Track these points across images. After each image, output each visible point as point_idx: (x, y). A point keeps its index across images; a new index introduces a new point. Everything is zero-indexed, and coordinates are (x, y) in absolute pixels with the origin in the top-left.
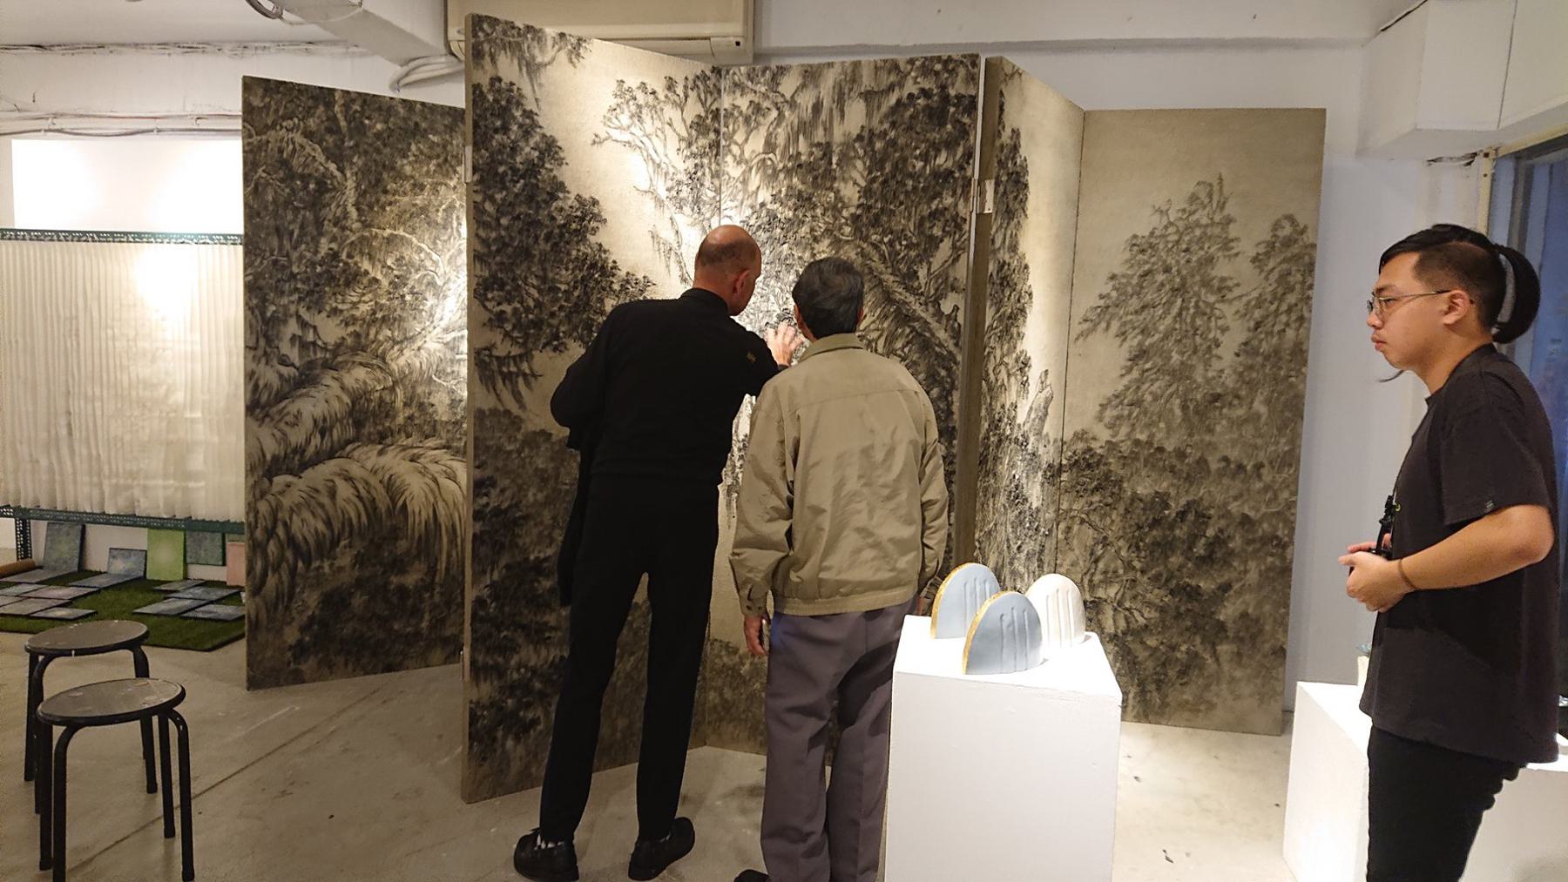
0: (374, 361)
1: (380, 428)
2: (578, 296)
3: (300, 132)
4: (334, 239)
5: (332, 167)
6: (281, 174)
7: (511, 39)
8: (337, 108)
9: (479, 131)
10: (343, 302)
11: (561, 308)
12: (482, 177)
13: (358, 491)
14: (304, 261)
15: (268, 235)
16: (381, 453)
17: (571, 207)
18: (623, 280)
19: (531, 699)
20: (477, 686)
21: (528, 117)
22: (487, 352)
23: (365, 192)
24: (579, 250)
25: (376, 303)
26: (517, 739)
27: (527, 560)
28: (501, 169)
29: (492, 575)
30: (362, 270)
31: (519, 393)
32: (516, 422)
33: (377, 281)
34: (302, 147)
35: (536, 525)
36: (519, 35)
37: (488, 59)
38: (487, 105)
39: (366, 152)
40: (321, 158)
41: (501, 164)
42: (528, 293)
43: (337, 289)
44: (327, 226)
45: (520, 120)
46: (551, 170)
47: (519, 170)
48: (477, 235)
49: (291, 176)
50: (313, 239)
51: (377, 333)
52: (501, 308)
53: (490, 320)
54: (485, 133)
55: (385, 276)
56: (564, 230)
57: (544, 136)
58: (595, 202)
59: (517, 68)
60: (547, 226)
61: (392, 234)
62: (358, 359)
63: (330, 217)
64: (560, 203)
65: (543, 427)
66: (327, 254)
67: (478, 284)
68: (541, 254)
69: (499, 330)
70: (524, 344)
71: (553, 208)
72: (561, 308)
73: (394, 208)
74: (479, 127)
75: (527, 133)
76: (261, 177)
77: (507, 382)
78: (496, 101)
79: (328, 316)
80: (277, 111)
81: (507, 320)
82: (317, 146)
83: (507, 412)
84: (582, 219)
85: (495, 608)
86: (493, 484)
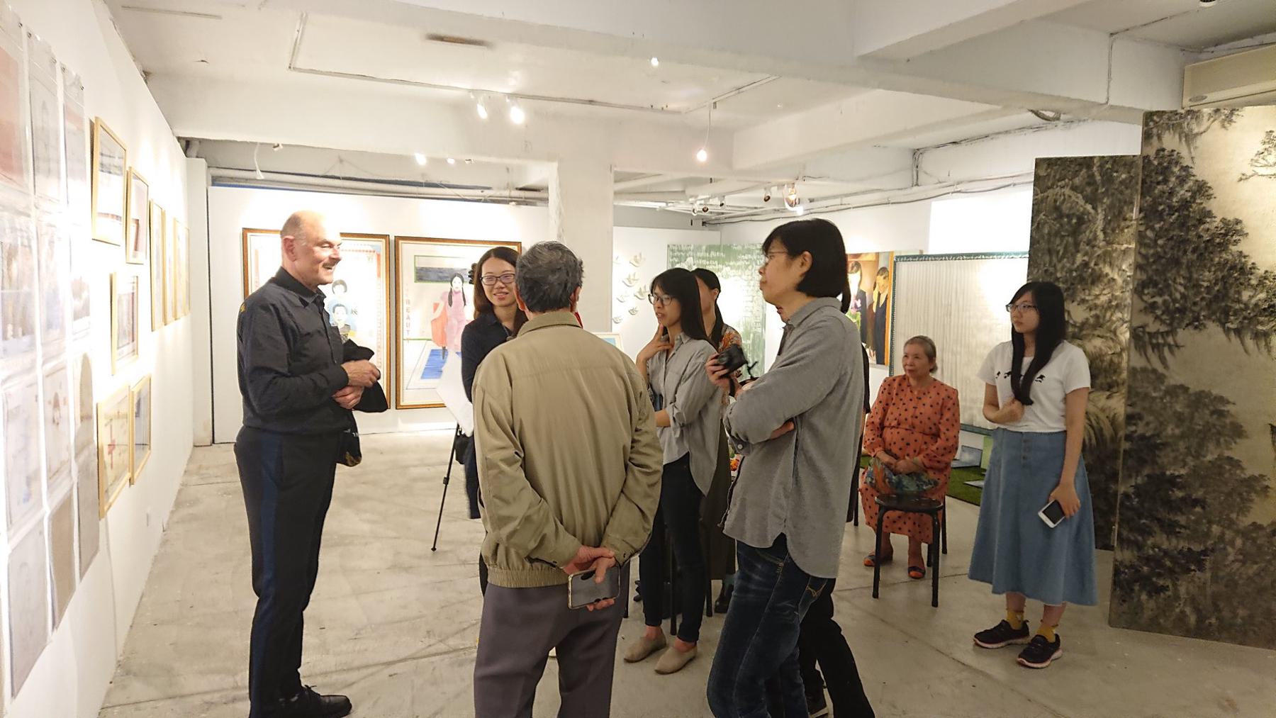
0: (1108, 335)
1: (1109, 380)
2: (1218, 291)
3: (1069, 187)
4: (1086, 254)
5: (1089, 207)
6: (1055, 215)
7: (1175, 122)
8: (1095, 169)
9: (1146, 185)
10: (1089, 295)
11: (1203, 299)
12: (1145, 214)
13: (1091, 422)
14: (1065, 269)
15: (1043, 254)
16: (1109, 397)
17: (1217, 227)
18: (1262, 277)
19: (1162, 571)
20: (1122, 551)
21: (1184, 171)
22: (1141, 329)
23: (1110, 221)
24: (1221, 257)
25: (1113, 295)
26: (1150, 595)
27: (1164, 473)
28: (1161, 208)
29: (1136, 479)
30: (1105, 273)
31: (1165, 358)
32: (1161, 378)
33: (1113, 280)
34: (1070, 197)
35: (1173, 451)
36: (1181, 118)
37: (1155, 138)
38: (1152, 168)
39: (1113, 194)
40: (1081, 202)
41: (1161, 204)
42: (1176, 290)
43: (1086, 287)
44: (1083, 246)
45: (1178, 173)
46: (1202, 203)
47: (1174, 207)
48: (1140, 253)
49: (1061, 216)
50: (1072, 255)
51: (1112, 315)
52: (1155, 299)
53: (1145, 308)
54: (1150, 186)
55: (1121, 276)
56: (1209, 244)
57: (1197, 181)
58: (1238, 222)
59: (1178, 140)
60: (1194, 242)
61: (1127, 248)
62: (1097, 333)
63: (1085, 240)
64: (1207, 226)
65: (1183, 382)
66: (1081, 264)
67: (1138, 285)
68: (1188, 262)
69: (1151, 315)
70: (1171, 324)
71: (1200, 230)
72: (1203, 299)
73: (1129, 229)
74: (1146, 183)
75: (1182, 181)
76: (1042, 219)
77: (1156, 350)
78: (1160, 164)
79: (1078, 304)
80: (1054, 176)
81: (1158, 308)
82: (1079, 195)
83: (1154, 371)
84: (1226, 235)
85: (1138, 502)
86: (1140, 418)
